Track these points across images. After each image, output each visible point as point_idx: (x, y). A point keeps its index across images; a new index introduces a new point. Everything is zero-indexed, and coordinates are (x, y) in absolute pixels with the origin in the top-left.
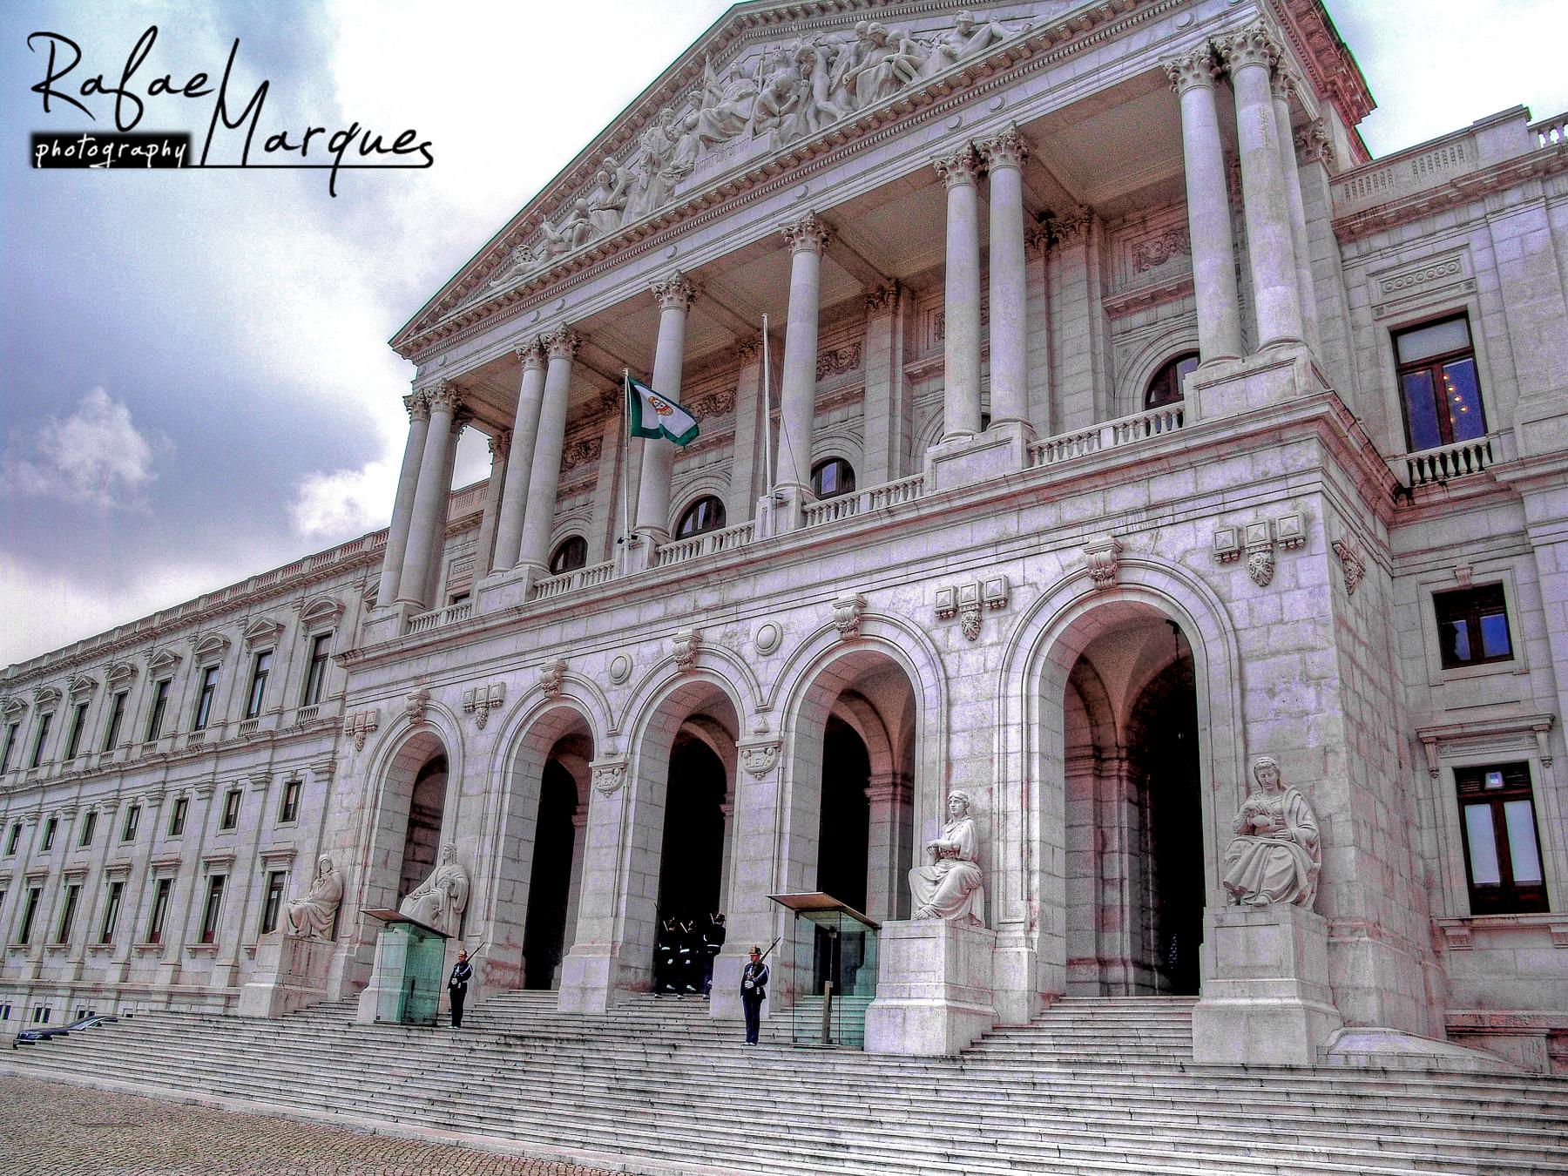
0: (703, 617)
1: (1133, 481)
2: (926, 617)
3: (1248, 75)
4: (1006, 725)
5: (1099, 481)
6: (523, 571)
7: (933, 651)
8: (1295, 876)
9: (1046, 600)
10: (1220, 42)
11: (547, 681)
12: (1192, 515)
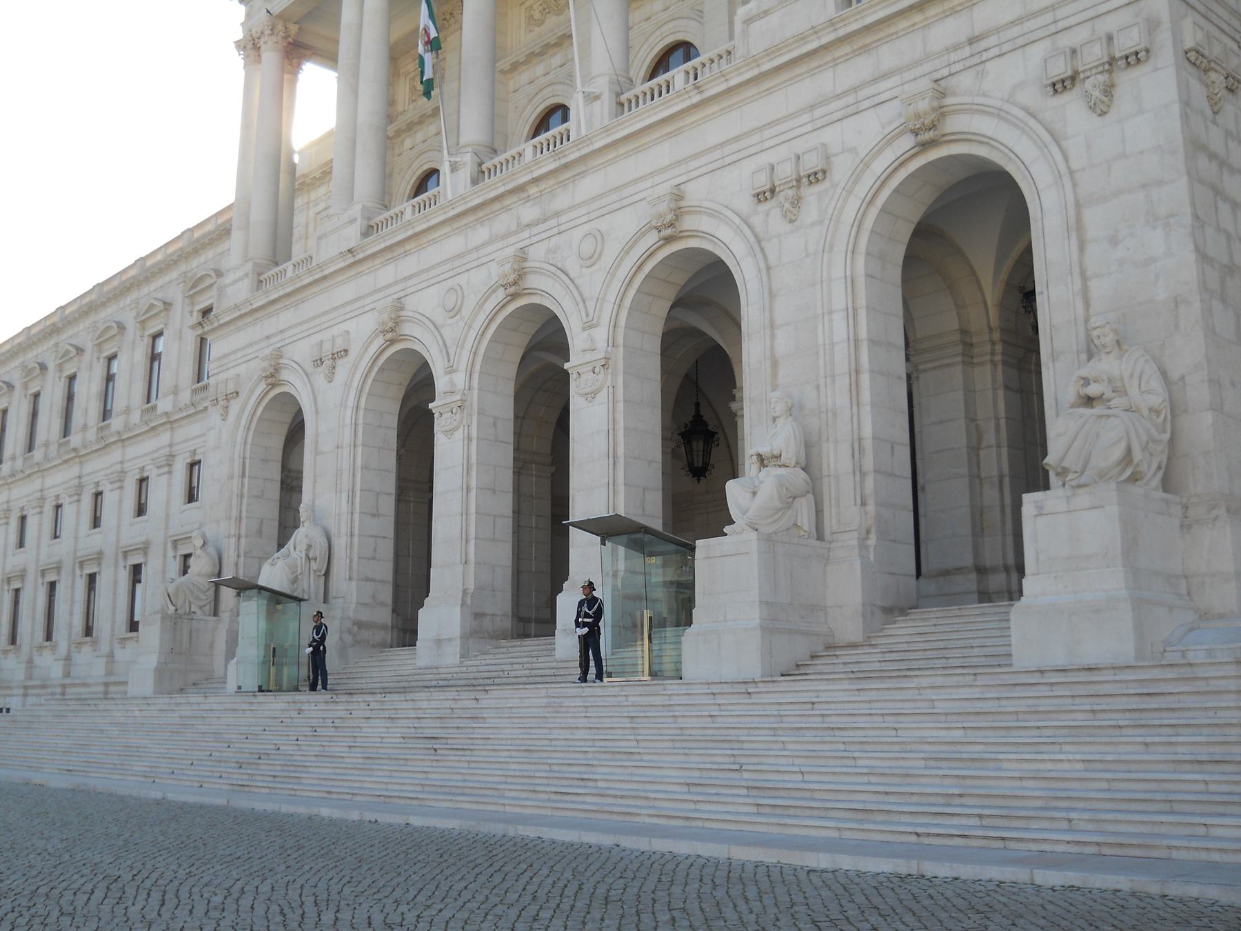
0: (526, 234)
2: (744, 203)
4: (831, 313)
7: (752, 239)
8: (1129, 451)
9: (865, 164)
12: (1020, 41)
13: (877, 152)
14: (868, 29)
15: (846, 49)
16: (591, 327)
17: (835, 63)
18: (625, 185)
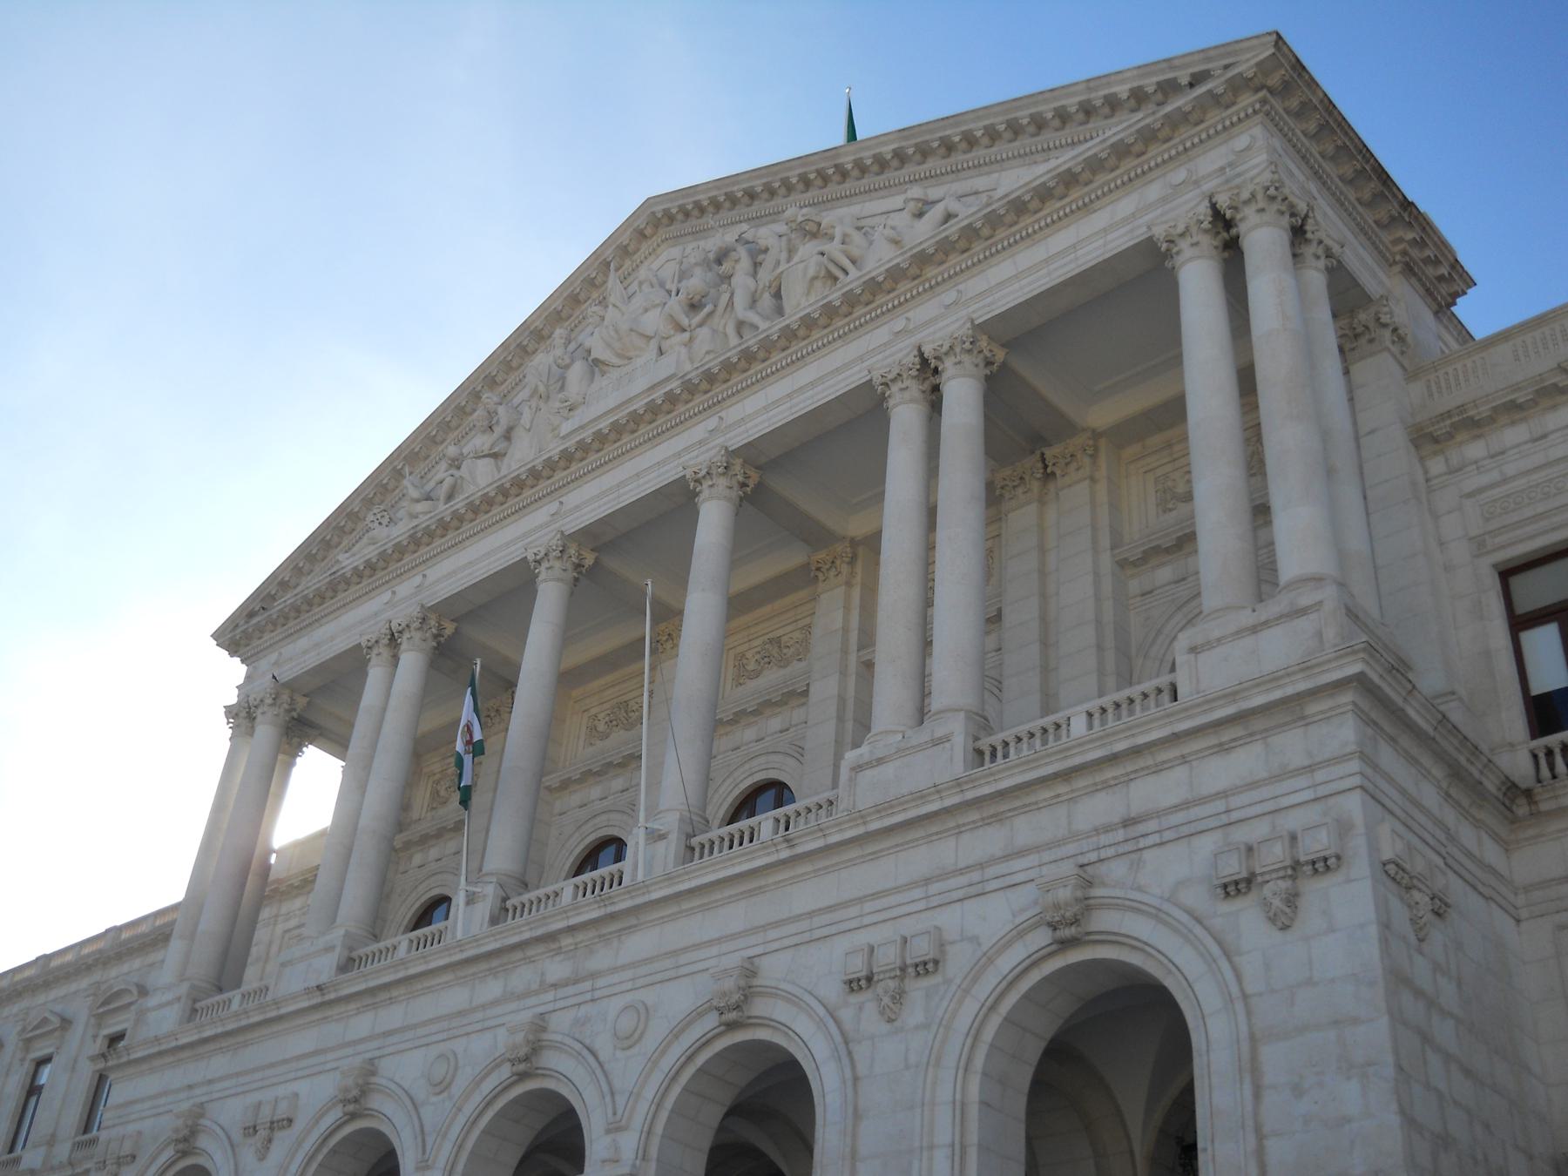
0: (550, 996)
1: (1106, 786)
2: (832, 990)
3: (1263, 240)
4: (931, 1147)
5: (1062, 789)
6: (337, 935)
7: (838, 1039)
9: (989, 959)
10: (1223, 201)
11: (347, 1090)
12: (1185, 830)
13: (1005, 944)
14: (1002, 794)
15: (974, 816)
16: (619, 1129)
17: (959, 831)
18: (685, 950)
